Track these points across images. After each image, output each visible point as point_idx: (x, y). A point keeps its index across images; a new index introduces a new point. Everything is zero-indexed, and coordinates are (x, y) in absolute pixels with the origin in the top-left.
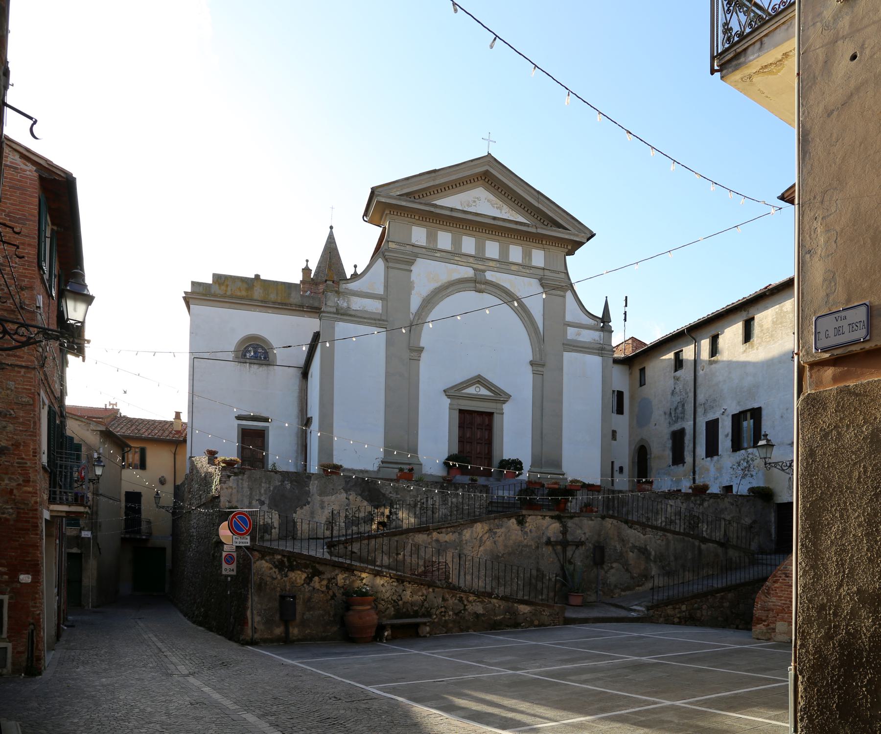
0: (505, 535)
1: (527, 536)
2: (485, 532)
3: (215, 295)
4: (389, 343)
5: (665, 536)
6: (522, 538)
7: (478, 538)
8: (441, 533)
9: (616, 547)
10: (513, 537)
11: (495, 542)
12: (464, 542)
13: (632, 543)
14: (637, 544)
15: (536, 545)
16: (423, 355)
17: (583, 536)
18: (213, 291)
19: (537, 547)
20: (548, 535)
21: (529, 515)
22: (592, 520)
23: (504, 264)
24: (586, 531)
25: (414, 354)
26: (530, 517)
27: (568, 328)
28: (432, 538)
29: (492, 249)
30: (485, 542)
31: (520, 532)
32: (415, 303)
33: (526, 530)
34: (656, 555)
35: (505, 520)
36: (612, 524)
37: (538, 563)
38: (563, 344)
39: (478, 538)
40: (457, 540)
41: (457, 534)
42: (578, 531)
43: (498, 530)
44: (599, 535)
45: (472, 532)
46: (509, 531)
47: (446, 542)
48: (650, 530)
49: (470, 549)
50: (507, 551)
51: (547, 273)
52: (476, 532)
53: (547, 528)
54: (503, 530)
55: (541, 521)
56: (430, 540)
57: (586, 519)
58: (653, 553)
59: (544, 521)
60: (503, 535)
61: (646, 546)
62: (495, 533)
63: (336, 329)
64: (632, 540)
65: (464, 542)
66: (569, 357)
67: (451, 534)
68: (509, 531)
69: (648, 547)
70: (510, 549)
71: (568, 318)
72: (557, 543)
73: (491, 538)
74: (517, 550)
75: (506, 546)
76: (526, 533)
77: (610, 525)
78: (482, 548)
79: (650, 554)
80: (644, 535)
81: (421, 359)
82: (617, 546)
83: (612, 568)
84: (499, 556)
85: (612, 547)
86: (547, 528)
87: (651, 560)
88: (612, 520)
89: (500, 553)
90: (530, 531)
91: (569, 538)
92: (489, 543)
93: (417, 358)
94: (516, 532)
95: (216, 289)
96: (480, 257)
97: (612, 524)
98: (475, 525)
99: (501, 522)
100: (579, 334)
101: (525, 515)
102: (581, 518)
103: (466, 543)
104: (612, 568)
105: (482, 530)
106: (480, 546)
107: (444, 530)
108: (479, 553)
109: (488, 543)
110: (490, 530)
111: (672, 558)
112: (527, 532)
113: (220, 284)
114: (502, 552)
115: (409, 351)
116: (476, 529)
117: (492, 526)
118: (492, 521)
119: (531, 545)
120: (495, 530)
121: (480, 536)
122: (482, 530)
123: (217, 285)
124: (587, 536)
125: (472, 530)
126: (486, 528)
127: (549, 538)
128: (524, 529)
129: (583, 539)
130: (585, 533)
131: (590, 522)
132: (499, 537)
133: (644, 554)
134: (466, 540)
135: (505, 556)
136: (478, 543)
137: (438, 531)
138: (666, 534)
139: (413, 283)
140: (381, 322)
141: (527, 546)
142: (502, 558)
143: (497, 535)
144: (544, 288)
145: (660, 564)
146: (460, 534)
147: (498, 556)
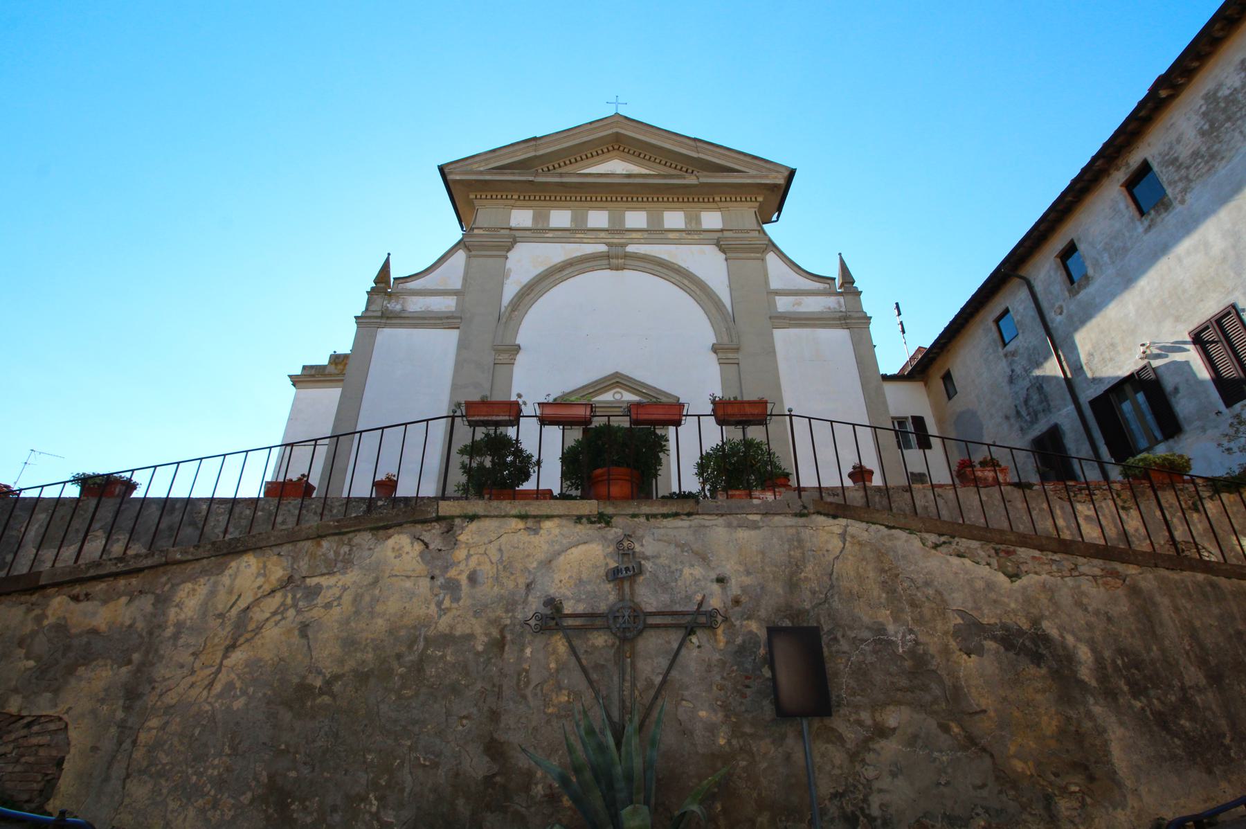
0: (357, 599)
1: (456, 599)
2: (267, 588)
3: (330, 375)
4: (462, 345)
5: (1115, 574)
6: (433, 608)
7: (234, 611)
8: (87, 596)
9: (880, 630)
10: (393, 606)
11: (304, 629)
12: (169, 632)
13: (961, 613)
14: (988, 617)
15: (495, 633)
16: (520, 358)
17: (716, 587)
18: (327, 372)
19: (499, 645)
20: (552, 591)
21: (473, 518)
22: (755, 526)
23: (656, 233)
24: (729, 567)
25: (504, 357)
26: (474, 526)
27: (777, 298)
28: (39, 619)
29: (636, 219)
30: (259, 628)
31: (425, 583)
32: (510, 291)
33: (452, 573)
34: (1099, 661)
35: (364, 538)
36: (843, 536)
37: (495, 716)
38: (770, 318)
39: (234, 611)
40: (140, 625)
41: (146, 603)
42: (687, 571)
43: (324, 581)
44: (793, 585)
45: (213, 593)
46: (376, 582)
47: (94, 632)
48: (1037, 553)
49: (185, 657)
50: (351, 664)
51: (727, 234)
52: (230, 592)
53: (548, 563)
54: (352, 577)
55: (524, 537)
56: (30, 627)
57: (721, 520)
58: (1084, 653)
59: (535, 539)
60: (347, 598)
61: (1035, 622)
62: (316, 591)
63: (379, 337)
64: (958, 599)
65: (169, 632)
66: (781, 336)
67: (124, 600)
68: (376, 582)
69: (1049, 628)
70: (370, 656)
71: (774, 284)
72: (592, 620)
73: (291, 613)
74: (399, 656)
75: (350, 643)
76: (452, 587)
77: (836, 544)
78: (238, 656)
79: (1069, 659)
80: (1013, 576)
81: (516, 362)
82: (891, 628)
83: (882, 732)
84: (310, 688)
85: (866, 634)
86: (548, 563)
87: (1082, 685)
88: (843, 521)
89: (319, 673)
90: (473, 579)
91: (649, 598)
92: (276, 631)
93: (508, 361)
94: (408, 584)
95: (332, 369)
96: (616, 230)
97: (843, 536)
98: (233, 564)
99: (346, 549)
100: (799, 304)
101: (452, 518)
102: (696, 520)
103: (176, 636)
104: (882, 732)
105: (260, 580)
106: (232, 647)
107: (102, 586)
108: (223, 678)
109: (272, 633)
110: (290, 579)
111: (1193, 675)
112: (458, 581)
113: (336, 364)
114: (330, 669)
115: (493, 353)
116: (234, 577)
117: (303, 565)
118: (308, 545)
119: (471, 637)
120: (312, 582)
121: (242, 604)
122: (260, 580)
123: (333, 366)
124: (734, 589)
125: (216, 584)
126: (278, 573)
127: (553, 604)
128: (446, 568)
129: (715, 603)
130: (721, 580)
131: (743, 534)
132: (328, 606)
133: (1037, 659)
134: (179, 625)
135: (337, 687)
136: (223, 634)
137: (77, 589)
138: (1119, 567)
139: (510, 270)
140: (449, 321)
141: (447, 639)
142: (326, 699)
143: (320, 600)
144: (725, 253)
145: (1138, 704)
146: (162, 601)
147: (304, 690)
